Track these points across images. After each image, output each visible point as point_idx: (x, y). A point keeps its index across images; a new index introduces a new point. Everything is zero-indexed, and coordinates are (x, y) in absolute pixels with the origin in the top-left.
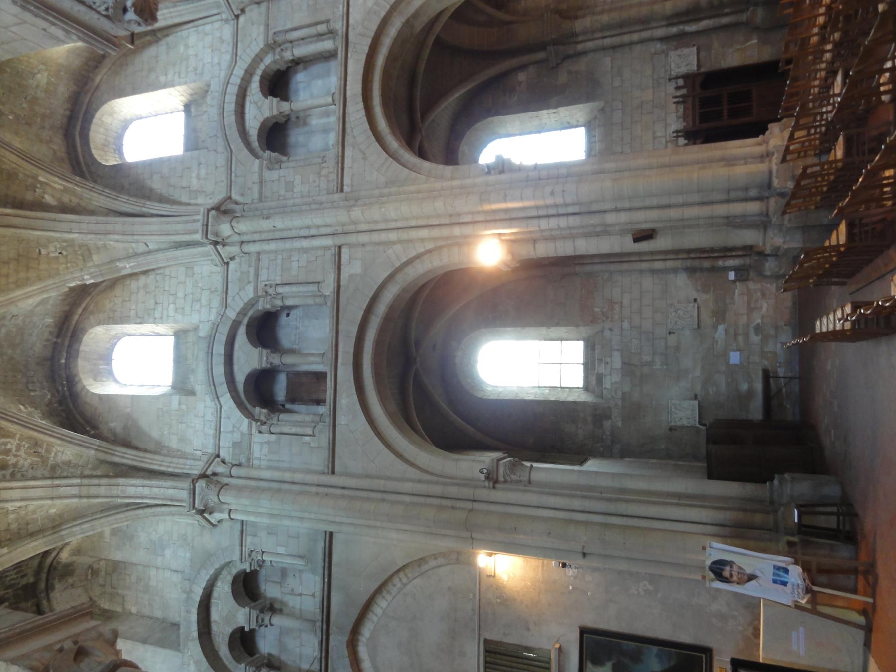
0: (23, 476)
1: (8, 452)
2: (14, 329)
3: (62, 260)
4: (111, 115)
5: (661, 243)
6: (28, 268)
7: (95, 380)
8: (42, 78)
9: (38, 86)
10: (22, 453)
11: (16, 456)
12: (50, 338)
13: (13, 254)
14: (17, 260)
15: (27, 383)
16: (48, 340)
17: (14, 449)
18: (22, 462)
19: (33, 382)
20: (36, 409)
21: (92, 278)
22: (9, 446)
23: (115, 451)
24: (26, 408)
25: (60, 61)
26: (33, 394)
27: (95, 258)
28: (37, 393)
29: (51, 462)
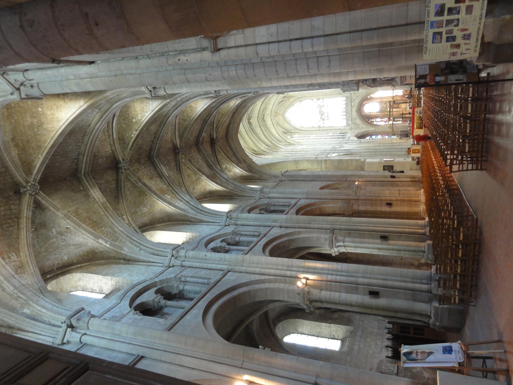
4: (151, 236)
5: (381, 302)
8: (145, 210)
9: (141, 210)
10: (13, 264)
12: (56, 265)
13: (95, 220)
16: (54, 265)
22: (12, 257)
25: (155, 210)
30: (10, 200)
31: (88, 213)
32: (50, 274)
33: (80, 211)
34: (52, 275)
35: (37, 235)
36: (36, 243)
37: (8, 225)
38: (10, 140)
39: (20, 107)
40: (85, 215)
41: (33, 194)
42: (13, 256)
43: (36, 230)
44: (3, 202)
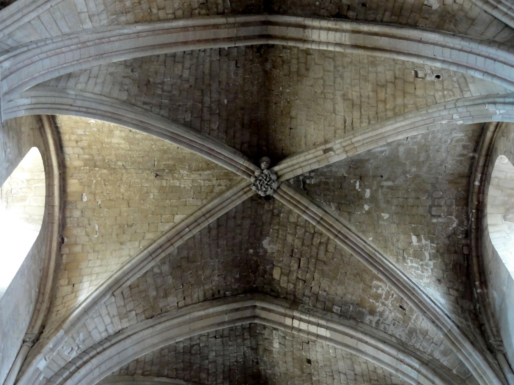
0: (385, 328)
1: (377, 297)
2: (415, 147)
3: (438, 86)
6: (405, 93)
7: (505, 218)
10: (389, 303)
11: (383, 304)
12: (465, 152)
13: (389, 76)
14: (394, 83)
15: (431, 207)
16: (463, 155)
17: (384, 296)
18: (387, 312)
19: (439, 206)
20: (432, 242)
21: (461, 118)
22: (380, 291)
23: (463, 346)
24: (419, 240)
26: (434, 220)
27: (471, 87)
28: (440, 220)
29: (410, 325)
30: (278, 215)
31: (366, 80)
32: (475, 177)
33: (354, 94)
34: (479, 176)
35: (374, 177)
36: (390, 183)
37: (322, 248)
38: (157, 182)
39: (90, 146)
40: (368, 89)
41: (275, 185)
42: (378, 287)
43: (361, 178)
44: (278, 230)
